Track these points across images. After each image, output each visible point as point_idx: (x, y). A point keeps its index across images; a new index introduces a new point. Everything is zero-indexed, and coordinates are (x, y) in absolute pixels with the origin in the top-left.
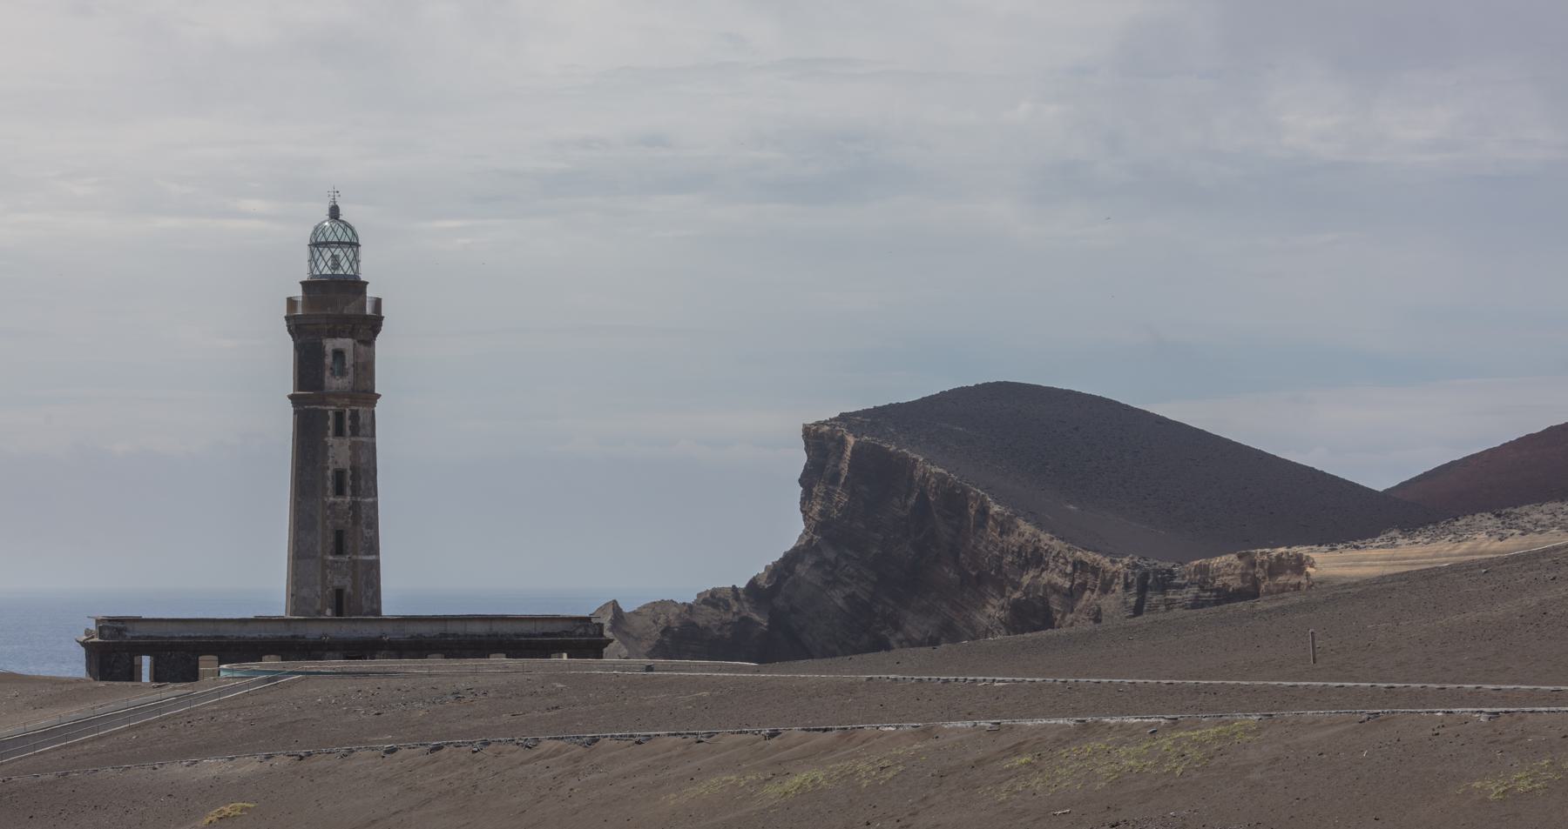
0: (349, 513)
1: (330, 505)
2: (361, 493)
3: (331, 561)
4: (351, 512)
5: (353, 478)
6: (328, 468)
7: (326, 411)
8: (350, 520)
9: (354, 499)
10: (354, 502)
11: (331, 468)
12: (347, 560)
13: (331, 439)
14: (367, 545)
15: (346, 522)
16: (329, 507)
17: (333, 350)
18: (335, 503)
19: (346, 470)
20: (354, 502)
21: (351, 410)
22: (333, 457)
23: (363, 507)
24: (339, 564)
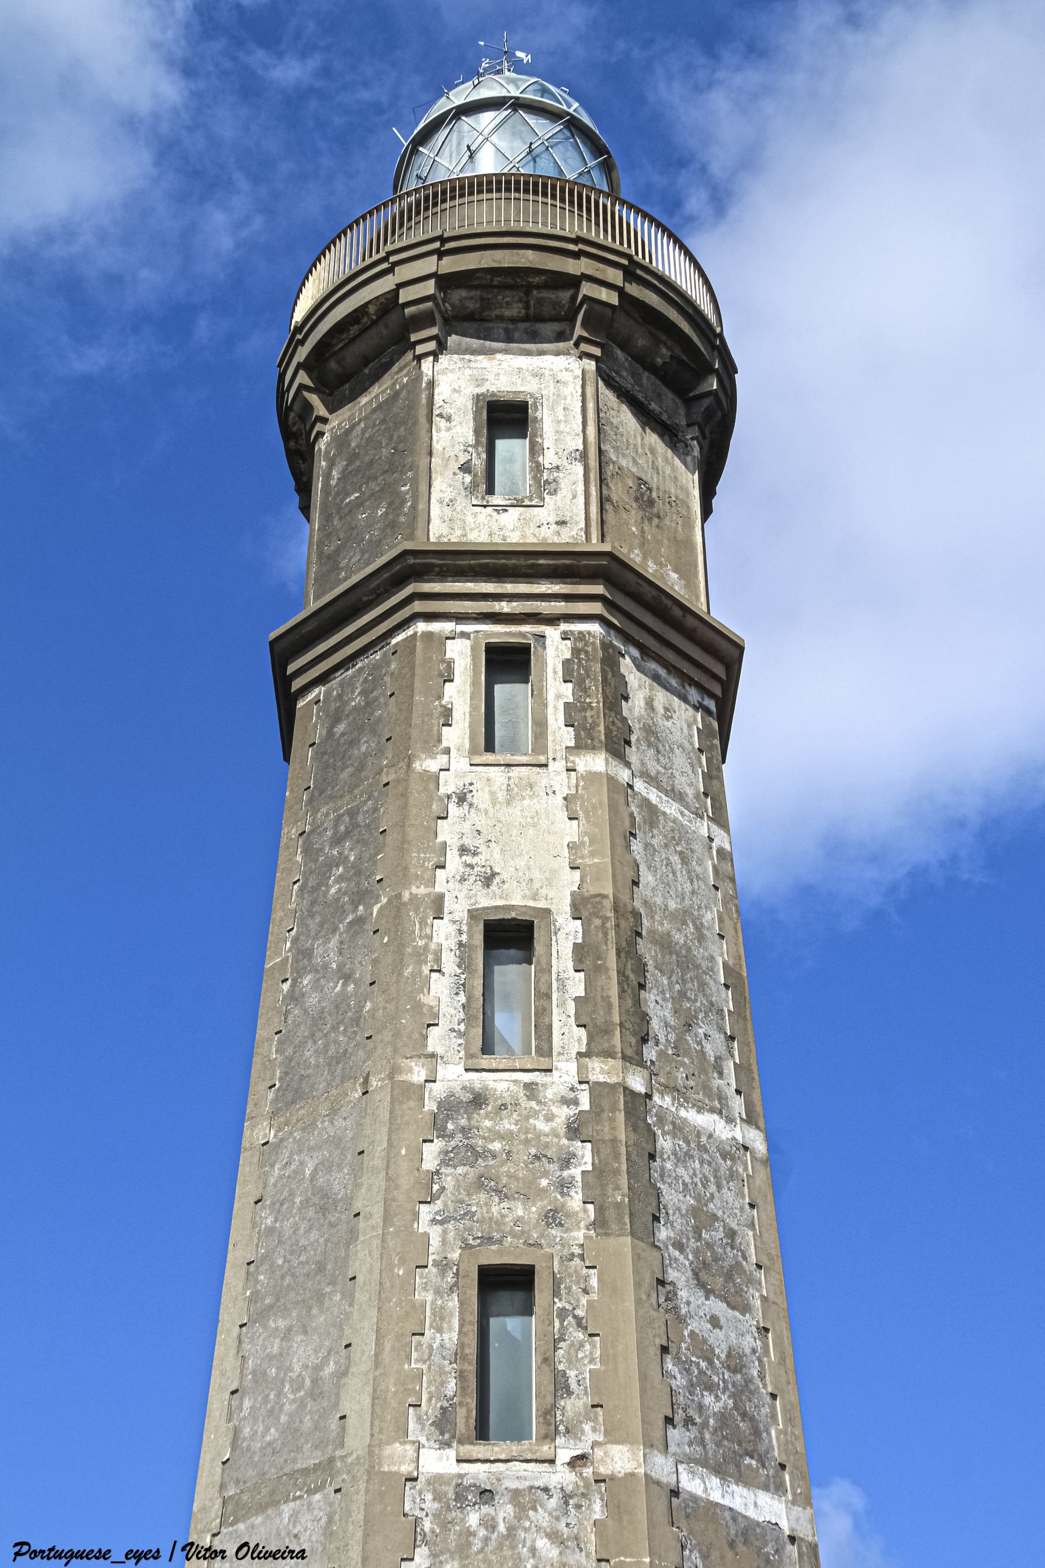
0: (567, 1161)
1: (449, 1106)
2: (650, 1053)
3: (437, 1481)
4: (585, 1153)
5: (581, 954)
6: (438, 906)
7: (438, 642)
8: (575, 1201)
9: (600, 1071)
10: (598, 1090)
11: (457, 907)
12: (561, 1477)
13: (460, 763)
14: (708, 1399)
15: (553, 1217)
16: (438, 1125)
17: (477, 398)
18: (478, 1100)
19: (548, 911)
20: (598, 1090)
21: (565, 637)
22: (463, 850)
23: (665, 1144)
24: (504, 1512)
